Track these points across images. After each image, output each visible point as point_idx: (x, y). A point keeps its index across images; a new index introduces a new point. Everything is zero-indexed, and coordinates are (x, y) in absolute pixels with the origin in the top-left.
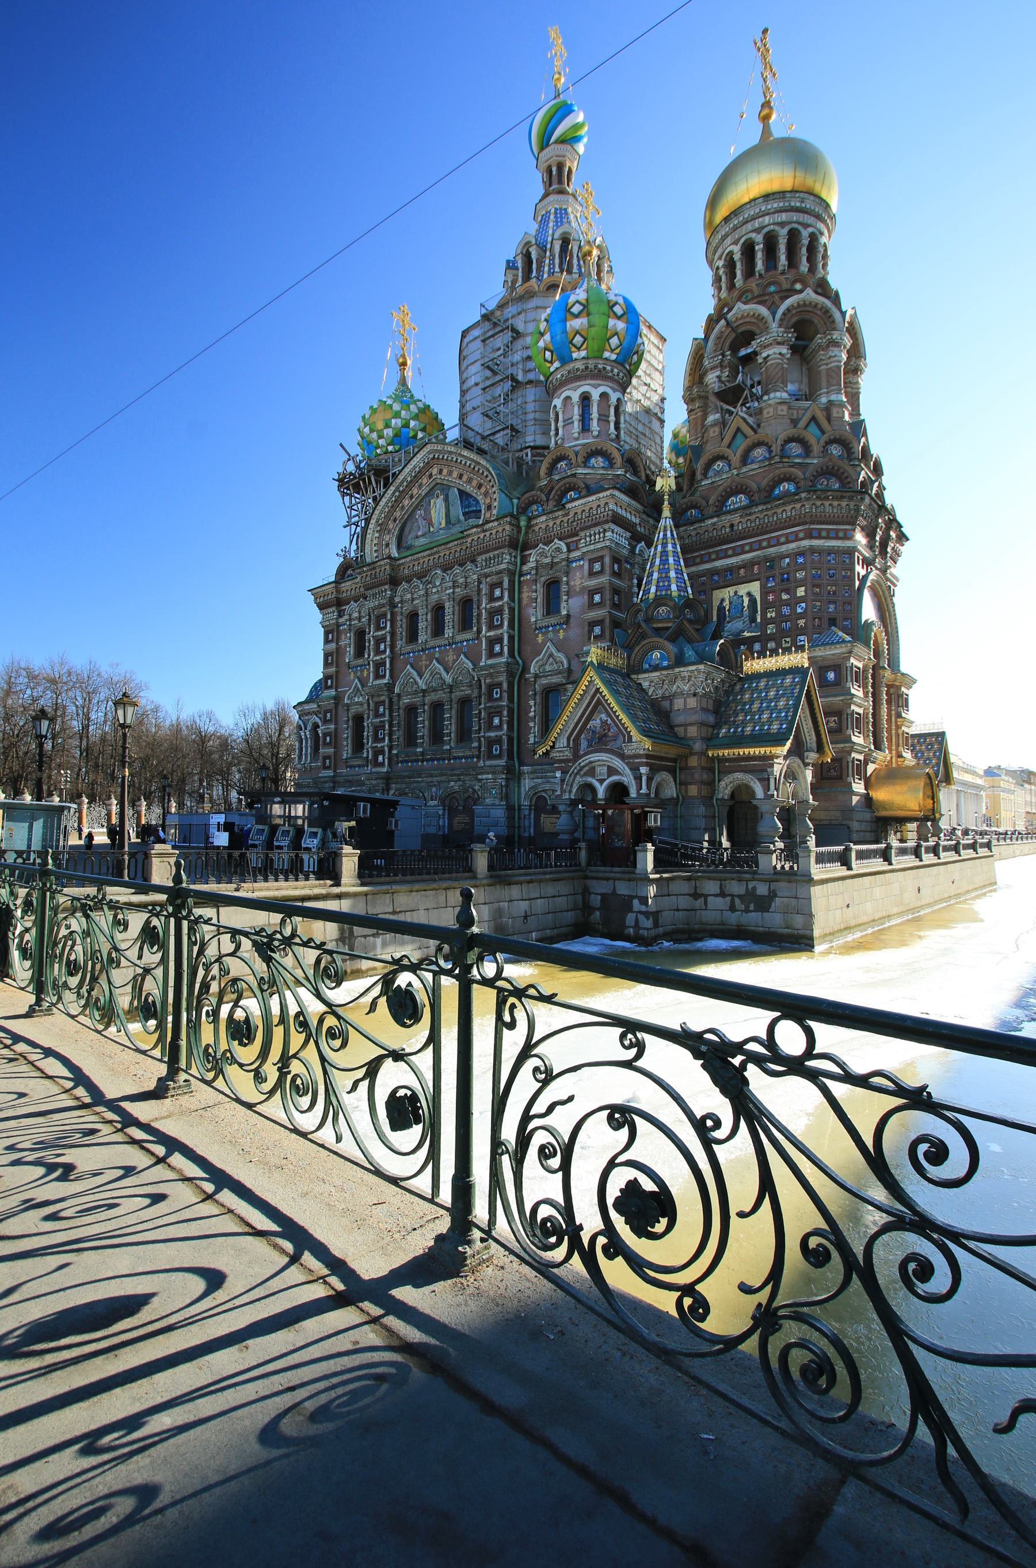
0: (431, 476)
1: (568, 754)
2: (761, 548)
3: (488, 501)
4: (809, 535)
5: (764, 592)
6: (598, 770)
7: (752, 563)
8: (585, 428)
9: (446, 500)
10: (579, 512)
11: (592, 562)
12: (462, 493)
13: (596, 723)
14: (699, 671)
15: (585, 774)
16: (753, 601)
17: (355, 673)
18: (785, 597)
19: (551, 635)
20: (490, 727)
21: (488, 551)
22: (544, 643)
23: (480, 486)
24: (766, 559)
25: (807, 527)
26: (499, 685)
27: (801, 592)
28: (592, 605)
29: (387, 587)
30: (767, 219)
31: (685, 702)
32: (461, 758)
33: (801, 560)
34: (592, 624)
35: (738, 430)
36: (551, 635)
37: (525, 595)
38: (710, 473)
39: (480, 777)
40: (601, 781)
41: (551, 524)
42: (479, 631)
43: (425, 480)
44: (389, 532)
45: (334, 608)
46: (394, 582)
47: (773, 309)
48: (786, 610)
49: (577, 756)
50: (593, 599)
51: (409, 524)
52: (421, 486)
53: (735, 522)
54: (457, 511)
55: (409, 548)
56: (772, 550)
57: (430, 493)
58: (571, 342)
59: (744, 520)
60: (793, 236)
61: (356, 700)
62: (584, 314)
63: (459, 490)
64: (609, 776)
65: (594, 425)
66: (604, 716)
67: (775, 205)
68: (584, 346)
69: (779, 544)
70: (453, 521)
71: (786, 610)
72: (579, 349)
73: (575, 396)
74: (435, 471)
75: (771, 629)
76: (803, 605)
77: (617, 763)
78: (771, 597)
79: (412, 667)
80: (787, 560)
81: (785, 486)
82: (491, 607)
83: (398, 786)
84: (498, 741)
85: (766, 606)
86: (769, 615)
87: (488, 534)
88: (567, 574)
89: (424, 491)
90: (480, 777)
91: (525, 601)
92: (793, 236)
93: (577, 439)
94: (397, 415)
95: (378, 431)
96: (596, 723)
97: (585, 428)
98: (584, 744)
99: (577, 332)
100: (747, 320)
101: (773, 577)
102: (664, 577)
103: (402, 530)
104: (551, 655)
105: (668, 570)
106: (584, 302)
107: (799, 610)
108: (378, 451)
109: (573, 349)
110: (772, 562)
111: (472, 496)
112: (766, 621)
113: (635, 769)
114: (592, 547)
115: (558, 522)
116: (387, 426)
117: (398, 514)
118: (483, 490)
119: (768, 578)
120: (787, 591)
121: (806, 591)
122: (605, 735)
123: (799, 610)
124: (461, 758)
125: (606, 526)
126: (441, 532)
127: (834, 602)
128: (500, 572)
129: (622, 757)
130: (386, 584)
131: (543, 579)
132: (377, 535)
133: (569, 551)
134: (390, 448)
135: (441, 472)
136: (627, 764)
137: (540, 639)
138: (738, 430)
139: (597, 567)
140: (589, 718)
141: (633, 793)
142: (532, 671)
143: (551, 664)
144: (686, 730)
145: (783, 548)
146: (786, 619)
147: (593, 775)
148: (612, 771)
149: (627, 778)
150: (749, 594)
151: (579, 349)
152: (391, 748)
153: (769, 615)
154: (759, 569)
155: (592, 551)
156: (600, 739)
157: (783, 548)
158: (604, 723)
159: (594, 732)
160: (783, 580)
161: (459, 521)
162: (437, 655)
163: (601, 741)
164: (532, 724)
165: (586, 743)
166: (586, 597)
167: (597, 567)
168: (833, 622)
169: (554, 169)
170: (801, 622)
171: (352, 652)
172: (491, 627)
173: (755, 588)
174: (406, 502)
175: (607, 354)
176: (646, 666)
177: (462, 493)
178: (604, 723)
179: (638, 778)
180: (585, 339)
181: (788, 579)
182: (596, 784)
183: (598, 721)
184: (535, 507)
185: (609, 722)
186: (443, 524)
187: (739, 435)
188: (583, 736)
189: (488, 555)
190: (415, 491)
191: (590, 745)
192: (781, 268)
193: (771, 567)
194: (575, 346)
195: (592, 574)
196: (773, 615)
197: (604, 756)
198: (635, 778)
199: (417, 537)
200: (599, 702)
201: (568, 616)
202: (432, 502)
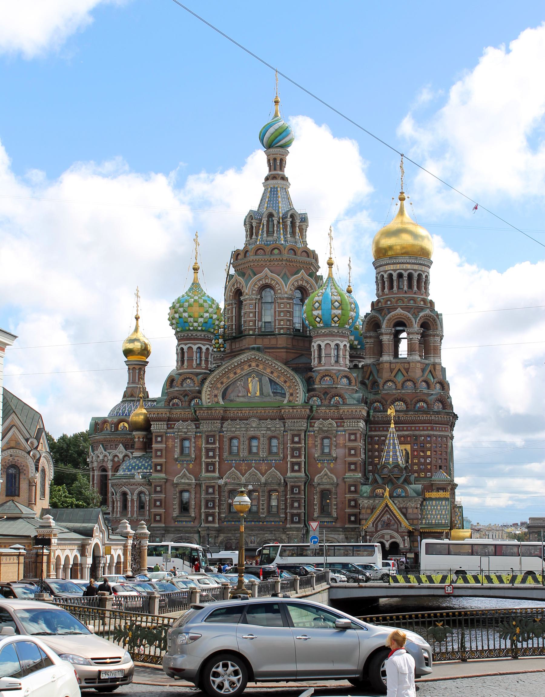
0: (250, 366)
1: (373, 529)
2: (411, 430)
3: (291, 391)
4: (432, 429)
5: (413, 450)
6: (386, 536)
7: (408, 436)
8: (337, 362)
9: (260, 381)
10: (346, 411)
11: (350, 434)
12: (271, 381)
13: (385, 518)
14: (419, 500)
15: (379, 538)
16: (407, 453)
17: (182, 465)
18: (422, 454)
19: (326, 465)
20: (292, 506)
21: (294, 419)
22: (322, 469)
23: (285, 382)
24: (414, 435)
25: (432, 425)
26: (299, 487)
27: (429, 453)
28: (350, 455)
29: (218, 421)
30: (409, 266)
31: (413, 510)
32: (272, 521)
33: (429, 439)
34: (350, 464)
35: (399, 370)
36: (326, 465)
37: (310, 442)
38: (386, 387)
39: (288, 533)
40: (387, 541)
41: (328, 411)
42: (285, 458)
43: (246, 367)
44: (217, 389)
45: (165, 423)
46: (223, 419)
47: (415, 315)
48: (422, 460)
49: (377, 531)
50: (350, 452)
51: (231, 387)
52: (242, 369)
53: (401, 416)
54: (268, 389)
55: (231, 401)
56: (417, 433)
57: (248, 375)
58: (332, 319)
59: (405, 416)
60: (420, 276)
61: (183, 481)
62: (333, 302)
63: (269, 378)
64: (391, 539)
65: (341, 360)
66: (389, 516)
67: (413, 261)
68: (338, 322)
69: (419, 430)
70: (265, 394)
71: (422, 460)
72: (335, 323)
73: (333, 345)
74: (254, 364)
75: (416, 467)
76: (430, 459)
77: (395, 534)
78: (416, 453)
79: (235, 468)
80: (423, 438)
81: (422, 404)
82: (293, 447)
83: (225, 535)
84: (298, 515)
85: (414, 457)
86: (415, 461)
87: (295, 410)
88: (335, 437)
89: (244, 372)
90: (288, 533)
91: (310, 445)
92: (420, 276)
93: (333, 366)
94: (207, 312)
95: (194, 318)
96: (385, 518)
97: (337, 362)
98: (380, 526)
99: (336, 316)
100: (402, 317)
101: (417, 444)
102: (395, 455)
103: (226, 389)
104: (326, 474)
105: (396, 451)
106: (340, 302)
107: (428, 461)
108: (191, 328)
109: (333, 322)
110: (417, 437)
111: (278, 384)
112: (413, 464)
113: (403, 537)
114: (351, 428)
115: (332, 411)
116: (202, 317)
117: (225, 380)
118: (288, 384)
119: (414, 444)
120: (423, 452)
121: (431, 453)
122: (389, 523)
123: (428, 461)
124: (272, 521)
125: (359, 420)
126: (256, 398)
127: (441, 459)
128: (301, 430)
129: (397, 532)
130: (218, 420)
131: (321, 436)
132: (210, 389)
133: (338, 426)
134: (200, 328)
135: (257, 366)
136: (399, 535)
137: (319, 465)
138: (399, 370)
139: (353, 437)
140: (382, 516)
141: (401, 546)
142: (315, 481)
143: (326, 479)
144: (413, 521)
145: (422, 433)
146: (422, 464)
147: (384, 539)
148: (392, 537)
149: (399, 540)
150: (405, 450)
151: (335, 323)
152: (219, 513)
153: (415, 461)
154: (410, 439)
155: (351, 430)
156: (387, 525)
157: (422, 433)
158: (389, 519)
159: (384, 522)
160: (421, 447)
161: (269, 395)
162: (253, 465)
163: (387, 525)
164: (315, 507)
165: (381, 526)
166: (347, 450)
167: (353, 437)
168: (440, 467)
169: (278, 162)
170: (429, 467)
171: (178, 451)
172: (293, 456)
173: (408, 447)
174: (232, 375)
175: (347, 326)
176: (395, 494)
177: (271, 381)
178: (389, 519)
179: (404, 540)
180: (339, 319)
181: (423, 447)
182: (385, 542)
183: (386, 518)
184: (315, 398)
185: (391, 518)
186: (258, 394)
187: (400, 373)
188: (379, 523)
189: (293, 421)
190: (238, 371)
191: (382, 527)
192: (414, 291)
193: (416, 439)
194: (334, 321)
195: (350, 440)
196: (417, 461)
197: (389, 531)
198: (403, 540)
199: (238, 396)
200: (387, 511)
201: (336, 458)
202: (250, 379)
